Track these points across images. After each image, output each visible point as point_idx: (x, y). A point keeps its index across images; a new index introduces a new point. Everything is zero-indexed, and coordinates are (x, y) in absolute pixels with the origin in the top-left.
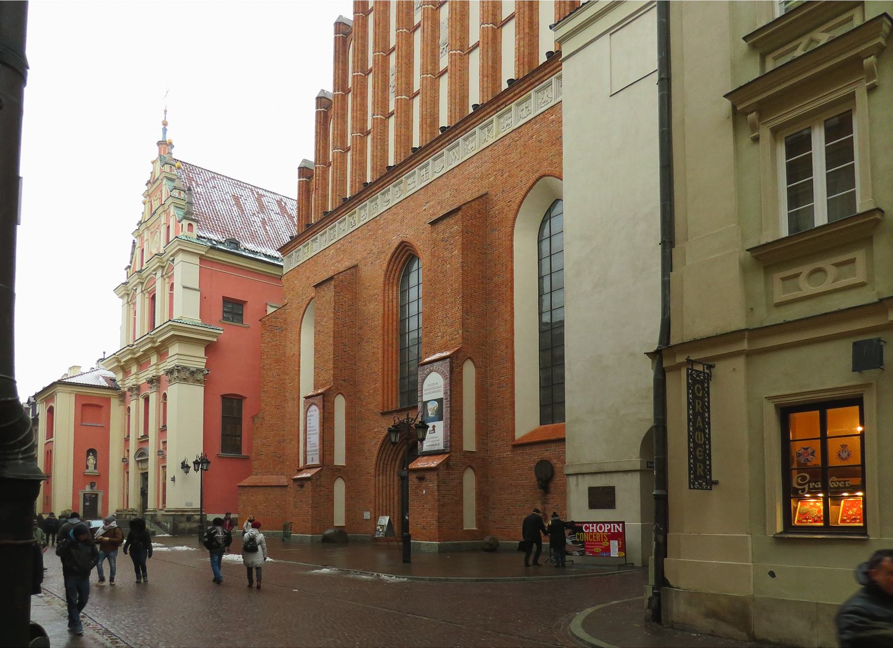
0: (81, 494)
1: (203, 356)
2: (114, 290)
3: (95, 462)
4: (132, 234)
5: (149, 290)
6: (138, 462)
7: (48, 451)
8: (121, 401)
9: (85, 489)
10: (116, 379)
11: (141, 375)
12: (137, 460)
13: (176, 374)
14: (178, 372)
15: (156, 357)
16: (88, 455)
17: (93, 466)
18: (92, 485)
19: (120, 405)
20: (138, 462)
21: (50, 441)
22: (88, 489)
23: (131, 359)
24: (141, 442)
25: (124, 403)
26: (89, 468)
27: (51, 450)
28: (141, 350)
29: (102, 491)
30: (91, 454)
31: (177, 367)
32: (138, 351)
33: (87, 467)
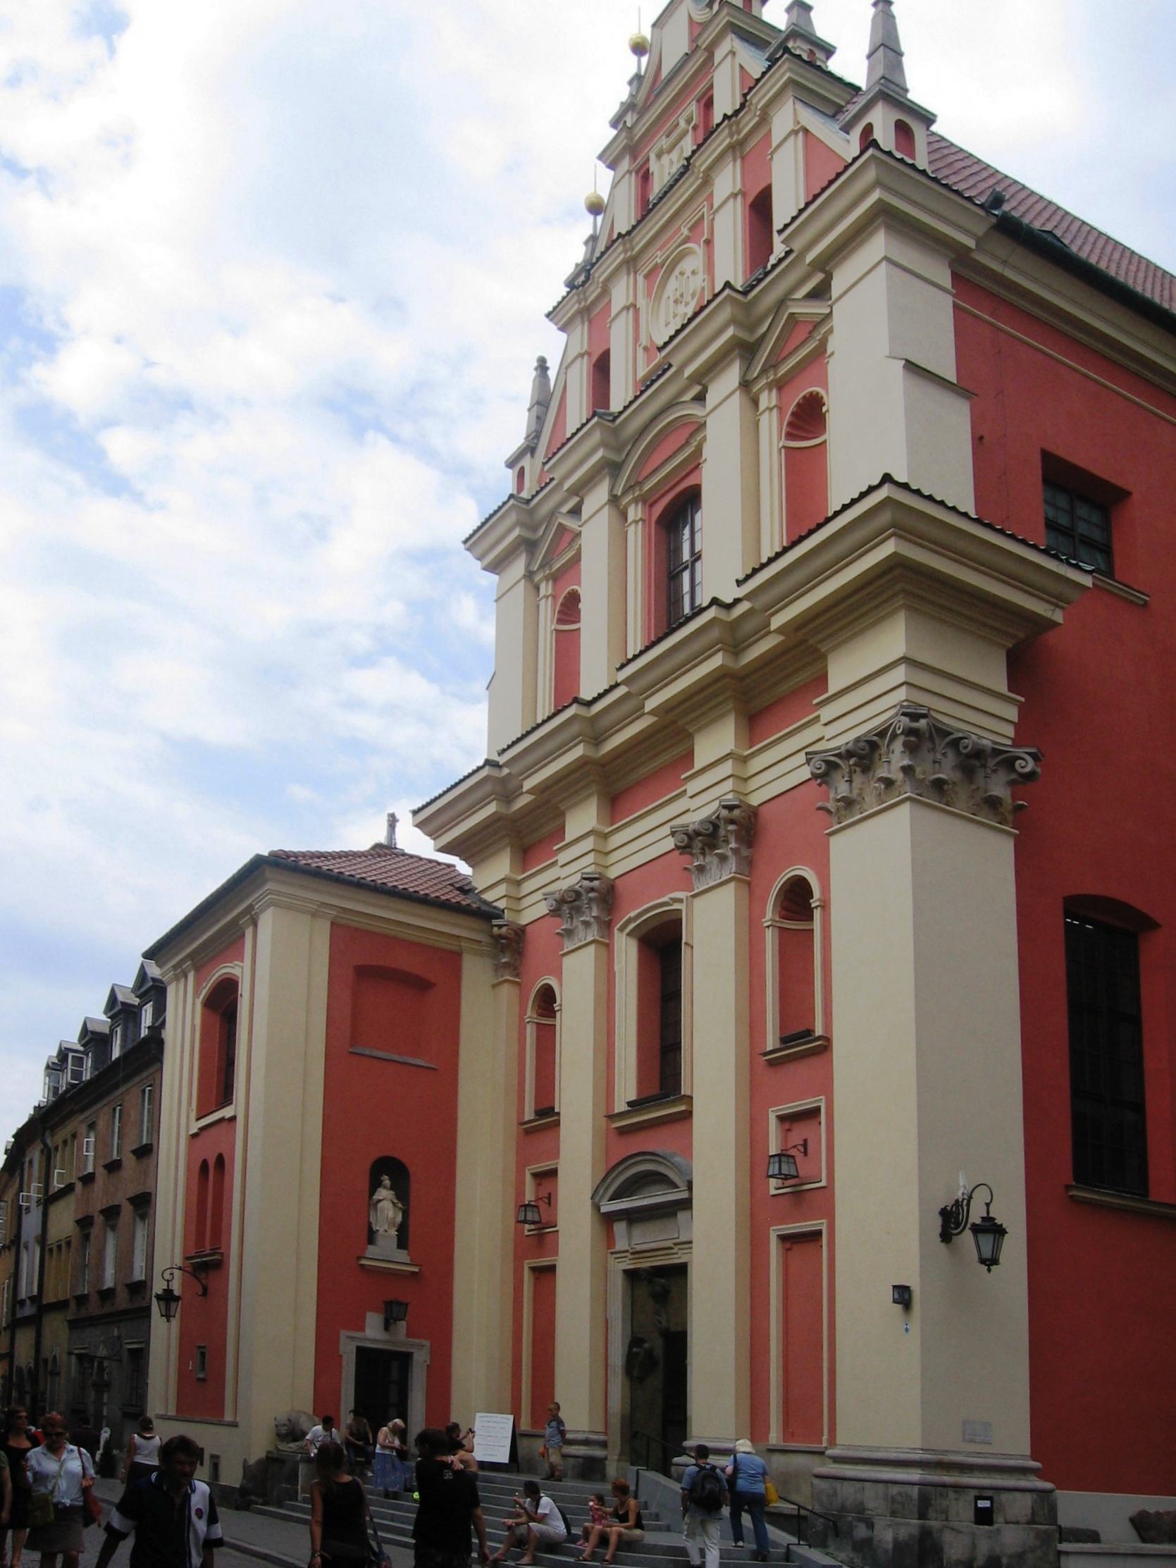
0: (348, 1352)
1: (1003, 687)
2: (465, 542)
3: (399, 1218)
4: (548, 315)
5: (647, 487)
6: (608, 1219)
7: (204, 1165)
8: (506, 965)
9: (362, 1329)
10: (474, 884)
11: (528, 887)
12: (603, 1210)
13: (896, 758)
14: (911, 749)
15: (733, 722)
16: (375, 1185)
17: (393, 1232)
18: (392, 1313)
19: (494, 986)
20: (608, 1219)
21: (222, 1120)
22: (373, 1331)
23: (582, 763)
24: (623, 1131)
25: (517, 975)
26: (380, 1241)
27: (220, 1160)
28: (651, 704)
29: (427, 1343)
30: (387, 1181)
31: (914, 717)
32: (763, 631)
33: (371, 1237)
